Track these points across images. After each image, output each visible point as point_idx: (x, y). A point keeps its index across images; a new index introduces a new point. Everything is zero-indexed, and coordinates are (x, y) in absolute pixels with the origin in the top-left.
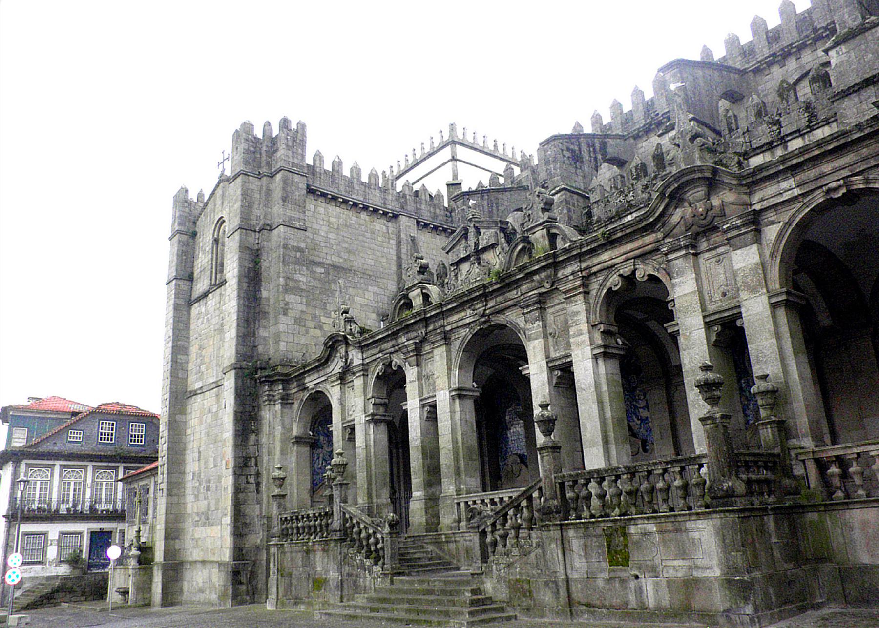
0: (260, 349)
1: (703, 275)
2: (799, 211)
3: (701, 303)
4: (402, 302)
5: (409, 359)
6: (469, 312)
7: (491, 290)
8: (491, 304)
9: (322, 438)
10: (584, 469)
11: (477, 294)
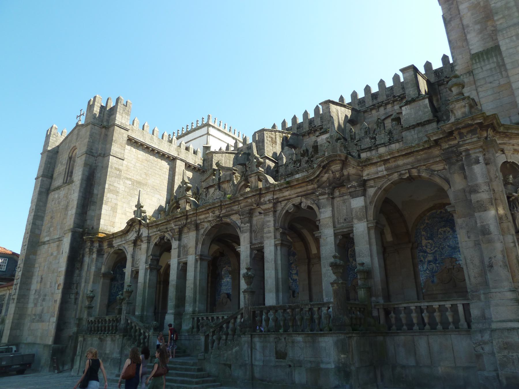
0: (88, 222)
1: (335, 208)
2: (386, 182)
3: (333, 223)
4: (175, 205)
5: (174, 236)
9: (118, 276)
10: (264, 304)
11: (217, 205)
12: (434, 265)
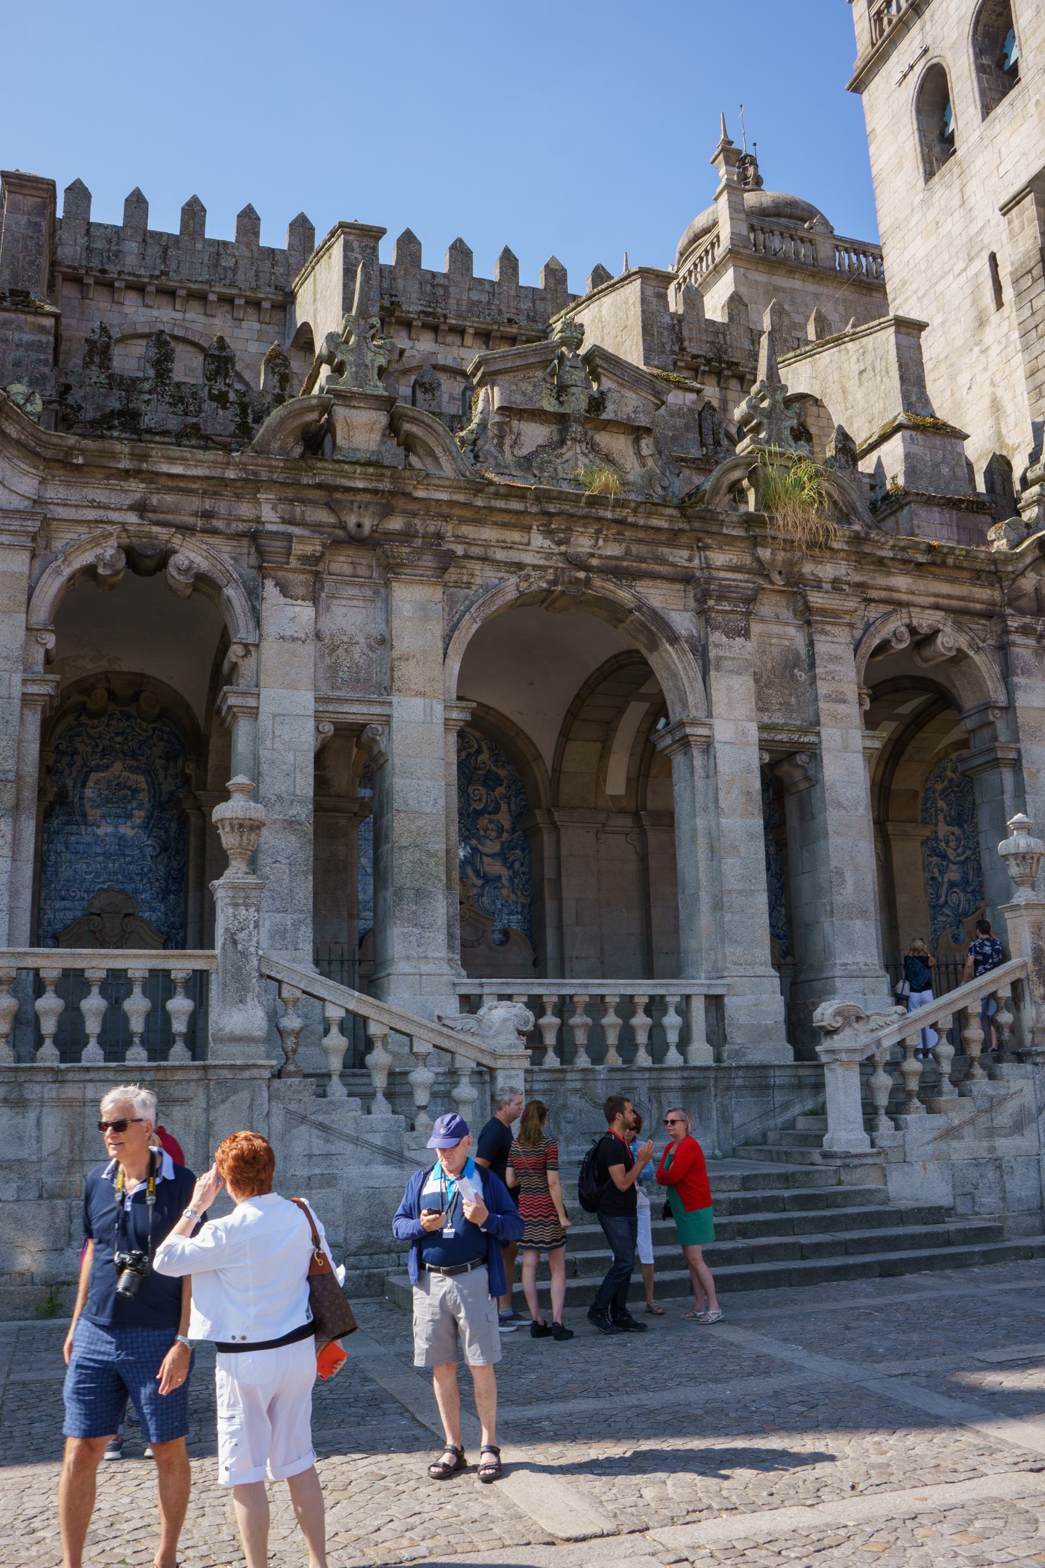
5: (280, 574)
6: (538, 540)
7: (642, 522)
11: (609, 515)
12: (962, 895)
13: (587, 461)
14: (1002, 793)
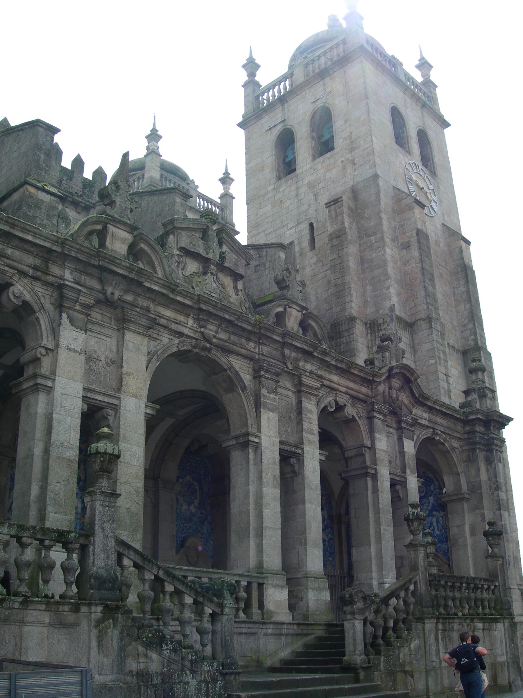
2: (424, 435)
4: (99, 227)
5: (71, 312)
6: (191, 322)
8: (223, 336)
11: (227, 317)
13: (215, 285)
14: (367, 490)
